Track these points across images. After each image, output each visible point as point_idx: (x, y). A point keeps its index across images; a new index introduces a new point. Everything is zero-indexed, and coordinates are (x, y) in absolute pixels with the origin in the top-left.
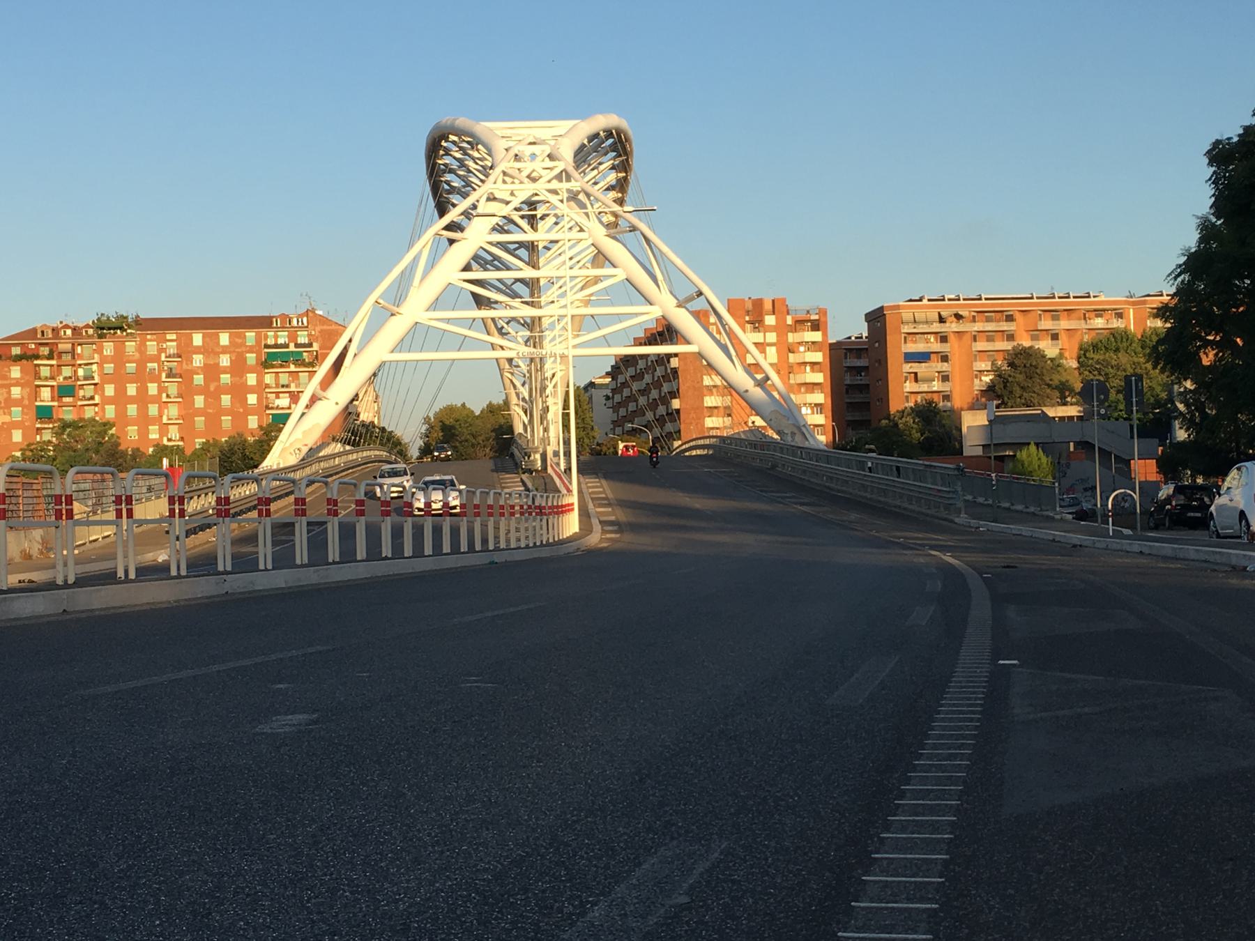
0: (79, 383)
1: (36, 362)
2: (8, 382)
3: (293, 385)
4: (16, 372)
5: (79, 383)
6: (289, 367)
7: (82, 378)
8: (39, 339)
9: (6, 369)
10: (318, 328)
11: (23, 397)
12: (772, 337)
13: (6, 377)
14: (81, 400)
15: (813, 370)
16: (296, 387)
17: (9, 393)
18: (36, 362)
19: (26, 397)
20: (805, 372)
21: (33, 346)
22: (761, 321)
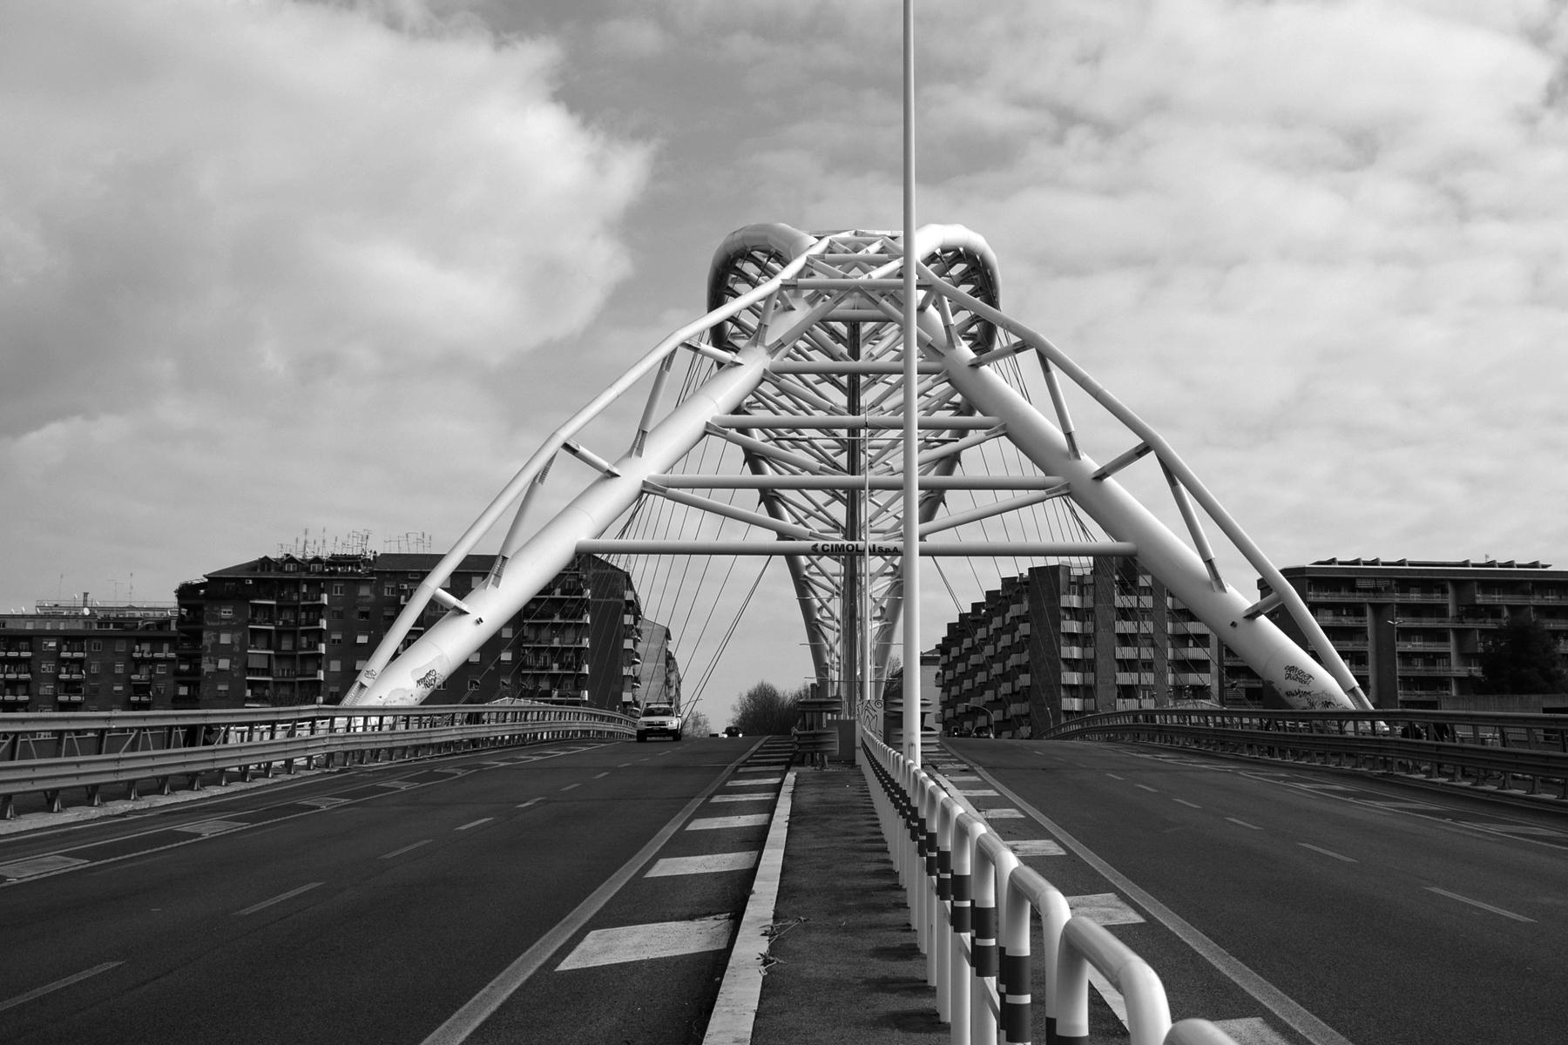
0: (301, 628)
1: (251, 602)
2: (218, 624)
3: (556, 640)
4: (226, 613)
5: (301, 628)
6: (552, 617)
7: (303, 622)
8: (259, 574)
9: (216, 608)
10: (592, 572)
11: (233, 643)
12: (1147, 601)
13: (216, 618)
14: (303, 649)
15: (1196, 645)
16: (560, 642)
17: (218, 638)
18: (251, 602)
19: (237, 642)
20: (1187, 646)
21: (251, 582)
22: (1134, 582)
